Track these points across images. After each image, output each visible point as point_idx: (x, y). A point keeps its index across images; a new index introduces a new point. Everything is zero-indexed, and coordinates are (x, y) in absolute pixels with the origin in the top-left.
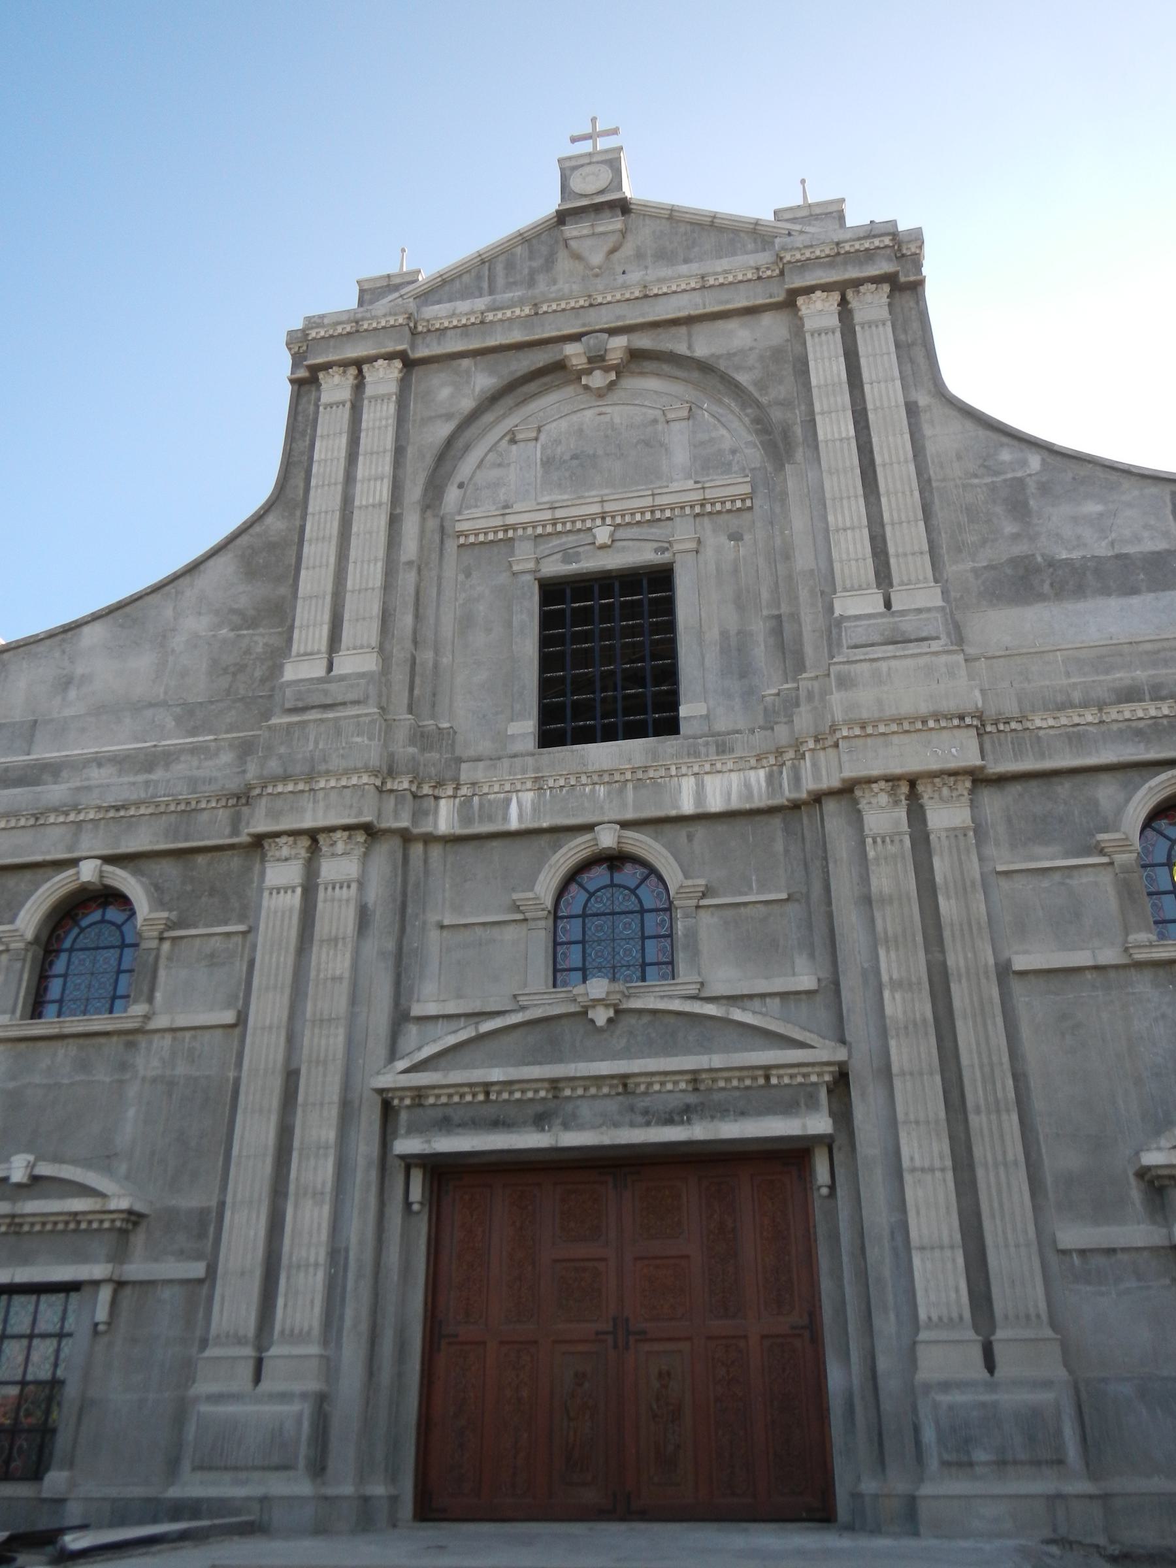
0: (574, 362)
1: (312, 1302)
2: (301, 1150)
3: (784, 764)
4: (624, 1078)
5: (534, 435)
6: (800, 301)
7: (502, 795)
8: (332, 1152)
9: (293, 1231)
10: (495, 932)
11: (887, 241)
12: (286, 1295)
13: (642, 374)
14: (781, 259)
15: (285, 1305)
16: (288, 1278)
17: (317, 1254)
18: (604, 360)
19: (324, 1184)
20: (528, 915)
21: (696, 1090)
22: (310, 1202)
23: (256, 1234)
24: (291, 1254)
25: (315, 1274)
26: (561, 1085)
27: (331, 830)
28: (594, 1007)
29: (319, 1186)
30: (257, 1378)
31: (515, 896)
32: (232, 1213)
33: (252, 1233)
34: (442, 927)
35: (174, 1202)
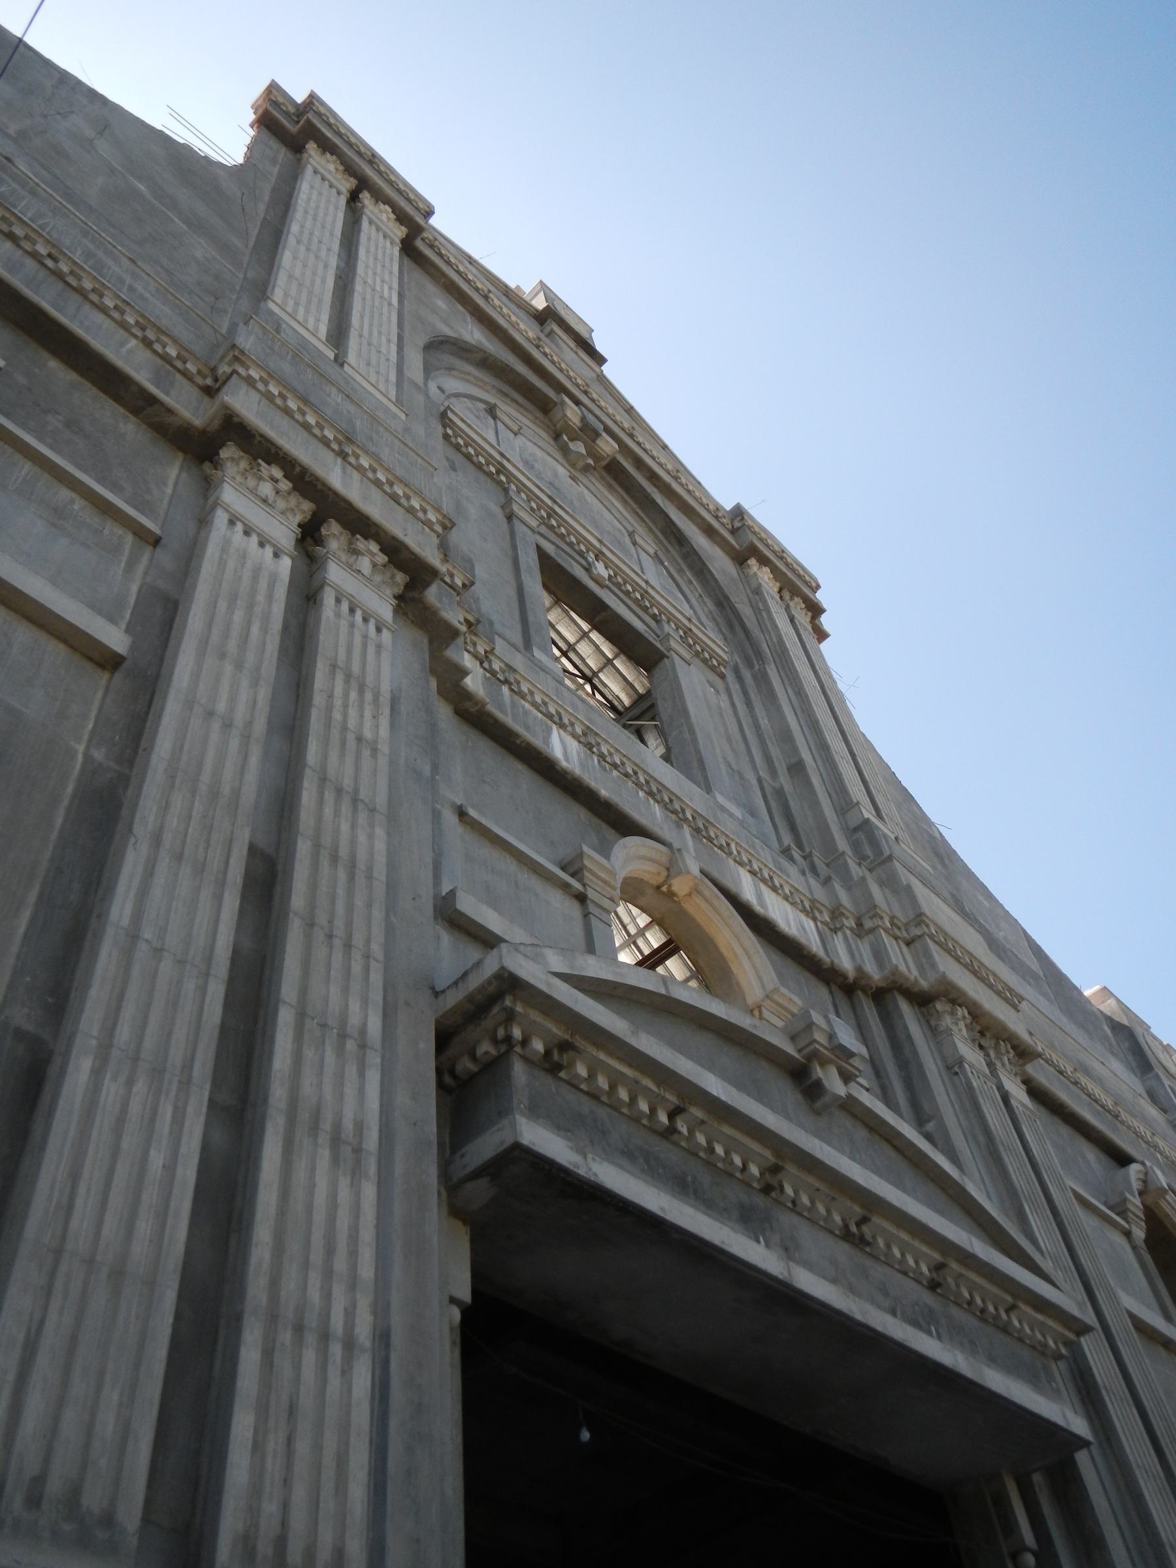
0: (569, 414)
2: (302, 1015)
3: (835, 931)
4: (872, 1203)
5: (516, 428)
6: (752, 562)
7: (540, 715)
8: (374, 1059)
10: (535, 883)
11: (814, 585)
12: (263, 1410)
13: (610, 487)
14: (743, 519)
15: (258, 1447)
16: (268, 1354)
17: (350, 1313)
18: (594, 441)
19: (359, 1127)
20: (591, 893)
21: (933, 1286)
22: (325, 1154)
23: (170, 1168)
24: (275, 1282)
27: (360, 526)
28: (824, 1063)
29: (348, 1125)
31: (585, 849)
32: (97, 1073)
33: (157, 1160)
34: (462, 814)
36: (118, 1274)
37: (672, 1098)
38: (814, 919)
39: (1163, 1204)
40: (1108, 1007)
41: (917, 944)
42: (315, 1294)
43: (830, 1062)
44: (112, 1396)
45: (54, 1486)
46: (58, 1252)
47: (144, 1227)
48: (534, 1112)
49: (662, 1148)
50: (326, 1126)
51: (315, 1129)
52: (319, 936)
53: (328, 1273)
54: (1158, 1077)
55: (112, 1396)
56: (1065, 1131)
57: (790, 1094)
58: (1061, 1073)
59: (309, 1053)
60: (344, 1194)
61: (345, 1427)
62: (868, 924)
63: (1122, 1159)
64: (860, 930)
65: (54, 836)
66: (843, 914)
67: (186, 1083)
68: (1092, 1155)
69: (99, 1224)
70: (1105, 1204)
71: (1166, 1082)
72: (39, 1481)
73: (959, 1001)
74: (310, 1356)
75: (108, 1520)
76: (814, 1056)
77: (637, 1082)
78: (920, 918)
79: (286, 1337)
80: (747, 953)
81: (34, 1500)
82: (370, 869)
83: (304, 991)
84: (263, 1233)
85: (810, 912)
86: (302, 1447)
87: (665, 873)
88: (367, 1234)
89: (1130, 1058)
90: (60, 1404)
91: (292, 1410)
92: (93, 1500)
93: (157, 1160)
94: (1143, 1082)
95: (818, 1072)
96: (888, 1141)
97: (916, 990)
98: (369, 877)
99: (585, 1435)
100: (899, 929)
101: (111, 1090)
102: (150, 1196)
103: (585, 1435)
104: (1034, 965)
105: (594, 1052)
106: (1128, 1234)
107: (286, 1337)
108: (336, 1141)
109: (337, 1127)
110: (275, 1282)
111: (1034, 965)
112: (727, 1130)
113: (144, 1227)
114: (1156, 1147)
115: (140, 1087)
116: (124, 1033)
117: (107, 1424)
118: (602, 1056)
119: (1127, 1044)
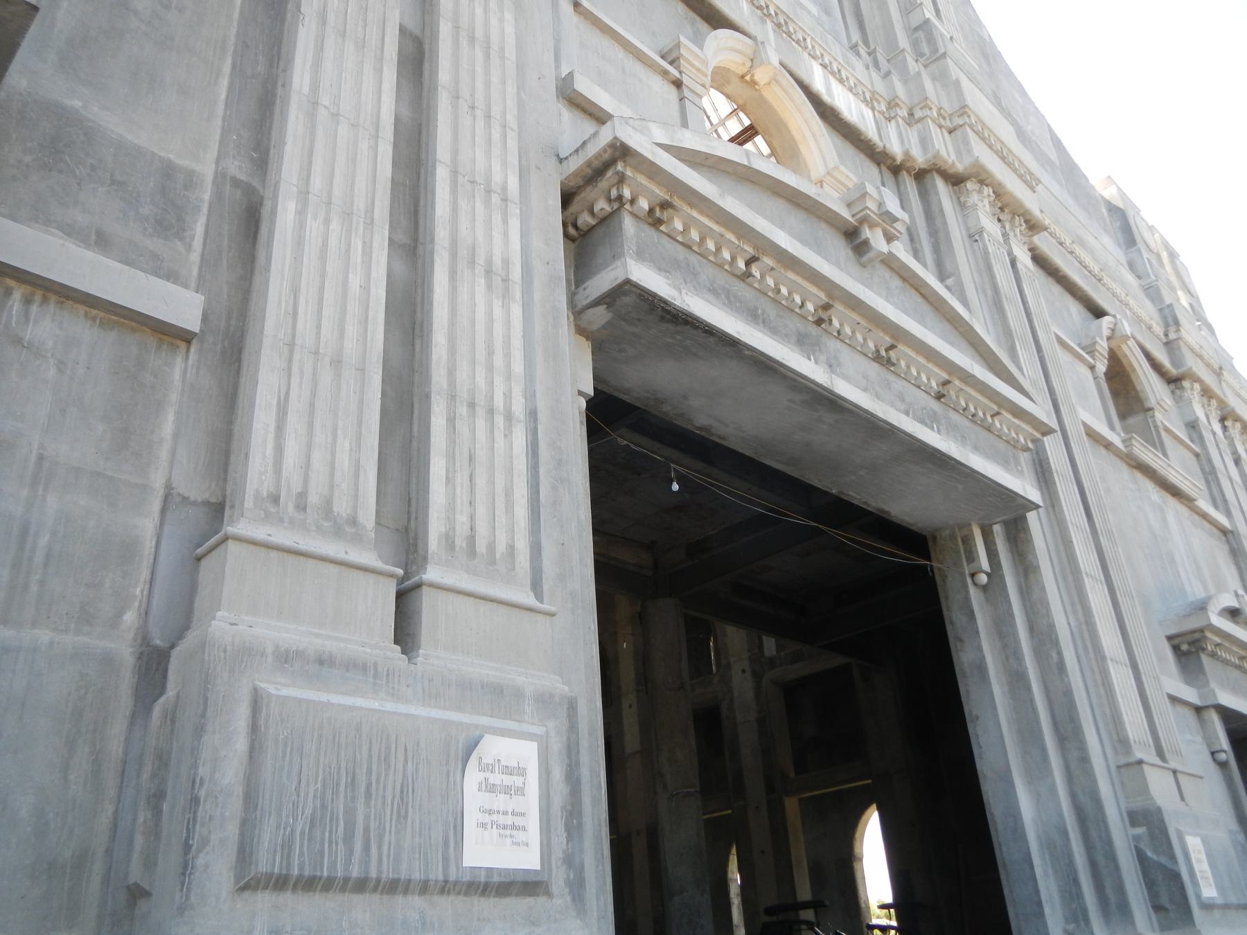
1: (509, 493)
2: (455, 173)
3: (889, 119)
4: (898, 335)
8: (514, 210)
9: (452, 323)
10: (639, 69)
12: (451, 457)
15: (449, 480)
16: (451, 420)
17: (508, 396)
20: (686, 80)
21: (939, 397)
22: (481, 282)
23: (366, 288)
24: (451, 373)
25: (507, 435)
26: (839, 307)
28: (872, 226)
29: (497, 261)
30: (405, 632)
31: (682, 39)
32: (301, 213)
33: (355, 281)
35: (77, 103)
36: (337, 363)
37: (750, 250)
38: (873, 109)
39: (1124, 347)
40: (1109, 193)
41: (958, 132)
42: (481, 381)
43: (877, 225)
44: (344, 445)
45: (313, 499)
46: (291, 345)
47: (352, 330)
48: (641, 255)
49: (738, 287)
50: (481, 260)
51: (472, 263)
52: (464, 107)
53: (490, 368)
54: (1139, 250)
55: (344, 445)
56: (1057, 289)
57: (842, 249)
58: (1061, 244)
59: (463, 204)
60: (498, 312)
61: (510, 471)
62: (918, 114)
63: (1098, 313)
64: (911, 119)
65: (236, 15)
66: (897, 105)
67: (370, 223)
68: (1075, 309)
69: (319, 327)
70: (1079, 345)
71: (1145, 255)
72: (303, 495)
73: (988, 181)
74: (481, 423)
75: (353, 521)
76: (864, 220)
77: (722, 236)
78: (963, 110)
79: (463, 410)
80: (814, 136)
81: (302, 507)
82: (502, 49)
83: (455, 153)
84: (439, 338)
85: (870, 103)
86: (481, 482)
87: (749, 64)
88: (517, 342)
89: (1119, 234)
90: (309, 446)
91: (471, 458)
92: (342, 507)
93: (355, 281)
94: (1126, 254)
95: (867, 233)
96: (916, 289)
97: (951, 171)
98: (502, 57)
99: (675, 487)
100: (944, 118)
101: (314, 227)
102: (353, 308)
103: (675, 487)
104: (1053, 154)
105: (689, 211)
106: (1092, 368)
107: (463, 410)
108: (489, 272)
109: (489, 262)
110: (451, 373)
111: (1053, 154)
112: (791, 275)
113: (352, 330)
114: (1127, 305)
115: (335, 225)
116: (317, 183)
117: (344, 462)
118: (695, 214)
119: (1118, 224)
